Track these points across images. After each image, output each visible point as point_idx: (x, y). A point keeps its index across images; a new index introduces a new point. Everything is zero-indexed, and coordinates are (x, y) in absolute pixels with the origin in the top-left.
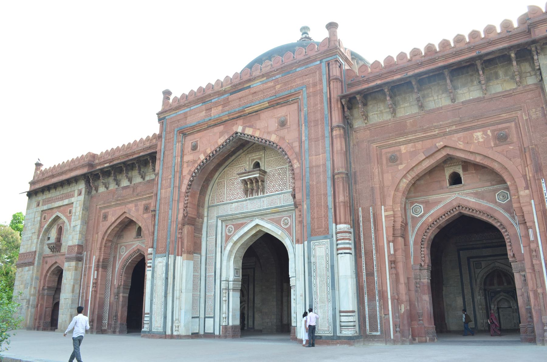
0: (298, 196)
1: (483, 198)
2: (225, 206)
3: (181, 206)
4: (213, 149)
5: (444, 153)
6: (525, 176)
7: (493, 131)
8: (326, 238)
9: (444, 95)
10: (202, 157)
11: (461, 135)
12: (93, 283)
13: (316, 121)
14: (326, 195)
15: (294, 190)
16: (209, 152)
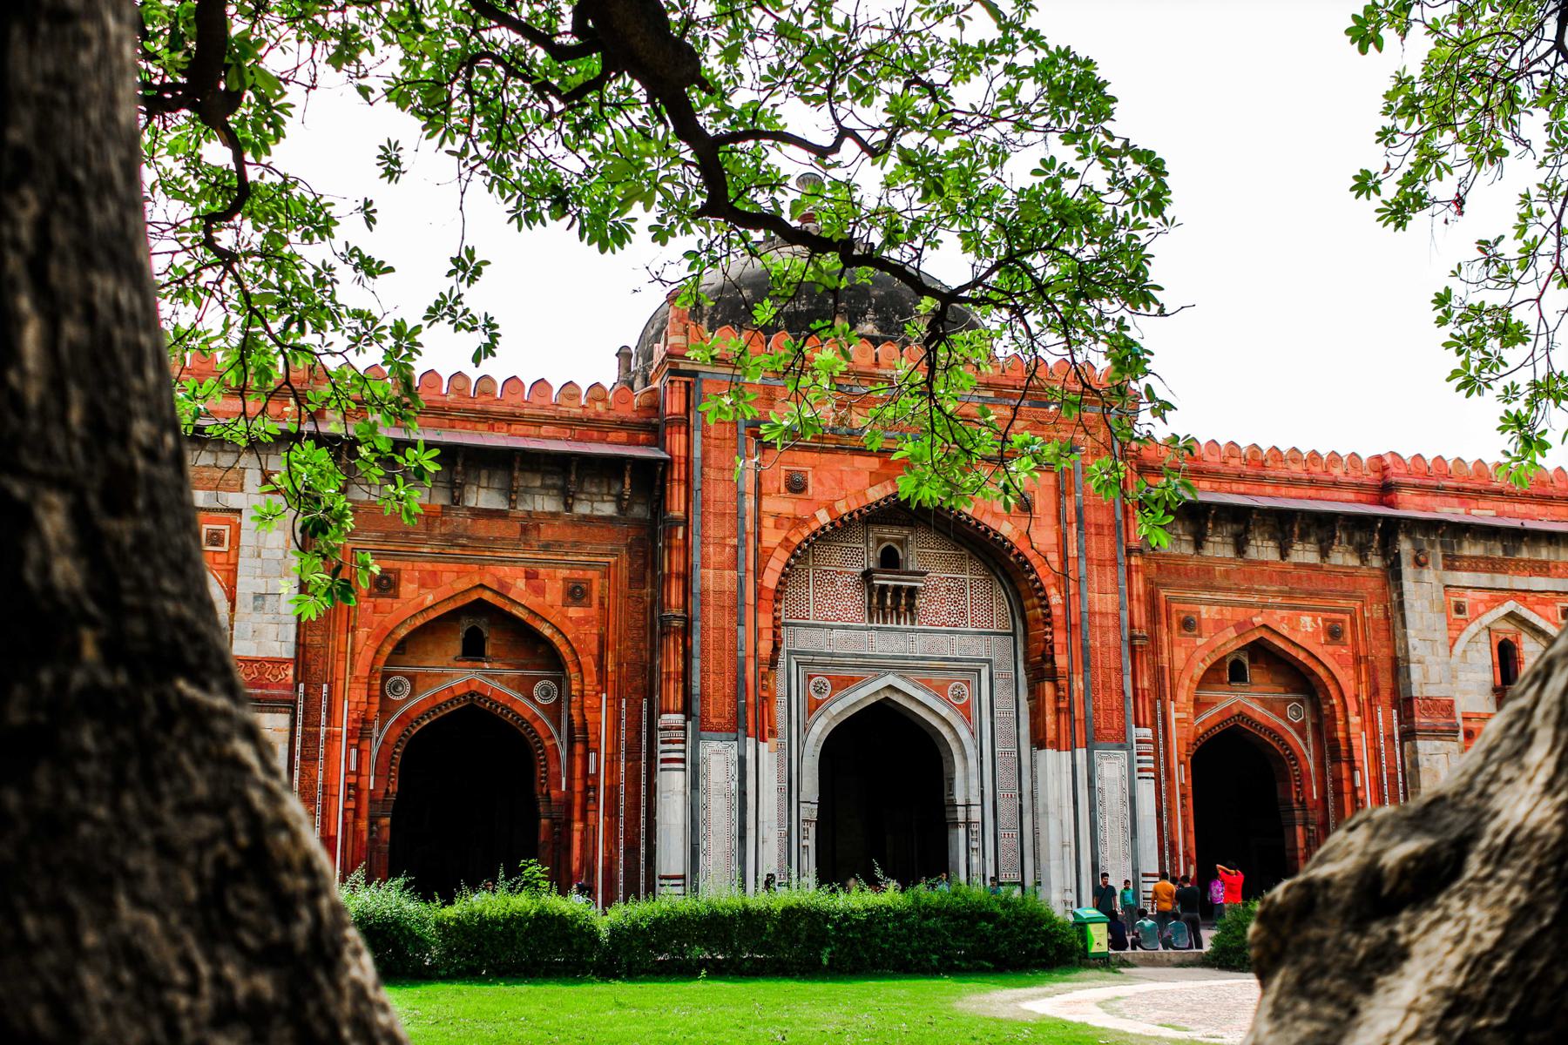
0: (1061, 661)
1: (1271, 709)
2: (814, 633)
3: (765, 621)
4: (854, 506)
5: (1256, 635)
6: (1357, 696)
7: (1324, 620)
8: (1121, 747)
9: (1271, 544)
10: (823, 517)
11: (1285, 613)
12: (348, 786)
13: (1099, 526)
14: (1120, 670)
15: (1052, 648)
16: (844, 511)
